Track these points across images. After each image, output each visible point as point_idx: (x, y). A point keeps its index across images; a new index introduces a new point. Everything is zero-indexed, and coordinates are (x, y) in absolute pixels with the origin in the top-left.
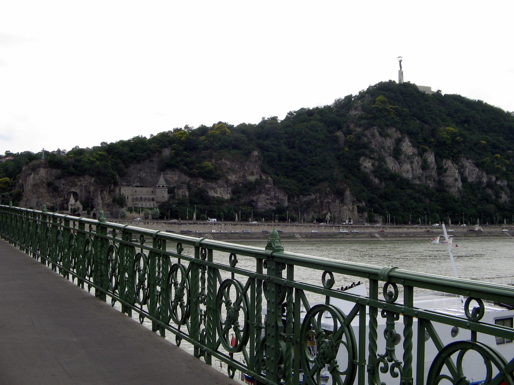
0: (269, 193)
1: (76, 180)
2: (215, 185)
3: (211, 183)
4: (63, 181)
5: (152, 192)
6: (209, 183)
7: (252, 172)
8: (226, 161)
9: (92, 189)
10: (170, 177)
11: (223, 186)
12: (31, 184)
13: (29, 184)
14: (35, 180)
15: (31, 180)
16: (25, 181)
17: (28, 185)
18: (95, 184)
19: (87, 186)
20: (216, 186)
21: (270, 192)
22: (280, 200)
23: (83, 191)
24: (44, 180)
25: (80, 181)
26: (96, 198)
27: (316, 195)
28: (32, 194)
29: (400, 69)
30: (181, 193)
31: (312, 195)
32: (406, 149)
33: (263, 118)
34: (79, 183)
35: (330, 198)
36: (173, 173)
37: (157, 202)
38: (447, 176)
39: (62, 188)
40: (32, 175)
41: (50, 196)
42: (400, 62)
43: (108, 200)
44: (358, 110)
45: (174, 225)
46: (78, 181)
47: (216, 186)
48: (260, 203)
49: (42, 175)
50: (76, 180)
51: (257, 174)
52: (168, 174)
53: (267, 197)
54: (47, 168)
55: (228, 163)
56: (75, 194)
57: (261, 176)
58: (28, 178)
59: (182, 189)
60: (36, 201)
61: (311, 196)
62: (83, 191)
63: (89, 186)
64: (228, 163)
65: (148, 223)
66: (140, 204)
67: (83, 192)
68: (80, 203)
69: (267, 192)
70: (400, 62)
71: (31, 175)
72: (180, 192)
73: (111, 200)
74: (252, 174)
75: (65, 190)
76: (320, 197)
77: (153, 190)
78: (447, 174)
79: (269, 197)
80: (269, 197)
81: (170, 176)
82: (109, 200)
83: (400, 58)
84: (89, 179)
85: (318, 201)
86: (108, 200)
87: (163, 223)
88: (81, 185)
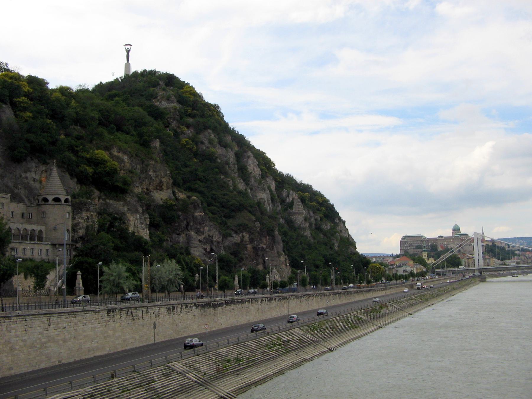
0: (201, 229)
2: (124, 206)
3: (115, 200)
5: (23, 215)
6: (111, 202)
7: (161, 182)
8: (120, 155)
10: (34, 180)
11: (137, 211)
20: (126, 209)
21: (204, 227)
22: (215, 244)
27: (241, 235)
29: (126, 62)
30: (82, 221)
31: (234, 235)
32: (253, 169)
33: (101, 83)
35: (265, 242)
36: (43, 168)
37: (54, 245)
38: (295, 213)
42: (128, 51)
44: (173, 102)
47: (126, 209)
48: (195, 249)
51: (167, 189)
52: (30, 171)
53: (199, 238)
55: (126, 158)
57: (174, 193)
59: (88, 210)
61: (231, 238)
64: (126, 158)
65: (173, 308)
66: (21, 247)
69: (199, 227)
70: (128, 51)
72: (82, 218)
74: (160, 187)
76: (252, 240)
77: (25, 212)
78: (294, 210)
79: (201, 238)
80: (201, 238)
81: (34, 176)
83: (129, 47)
85: (249, 246)
87: (195, 305)
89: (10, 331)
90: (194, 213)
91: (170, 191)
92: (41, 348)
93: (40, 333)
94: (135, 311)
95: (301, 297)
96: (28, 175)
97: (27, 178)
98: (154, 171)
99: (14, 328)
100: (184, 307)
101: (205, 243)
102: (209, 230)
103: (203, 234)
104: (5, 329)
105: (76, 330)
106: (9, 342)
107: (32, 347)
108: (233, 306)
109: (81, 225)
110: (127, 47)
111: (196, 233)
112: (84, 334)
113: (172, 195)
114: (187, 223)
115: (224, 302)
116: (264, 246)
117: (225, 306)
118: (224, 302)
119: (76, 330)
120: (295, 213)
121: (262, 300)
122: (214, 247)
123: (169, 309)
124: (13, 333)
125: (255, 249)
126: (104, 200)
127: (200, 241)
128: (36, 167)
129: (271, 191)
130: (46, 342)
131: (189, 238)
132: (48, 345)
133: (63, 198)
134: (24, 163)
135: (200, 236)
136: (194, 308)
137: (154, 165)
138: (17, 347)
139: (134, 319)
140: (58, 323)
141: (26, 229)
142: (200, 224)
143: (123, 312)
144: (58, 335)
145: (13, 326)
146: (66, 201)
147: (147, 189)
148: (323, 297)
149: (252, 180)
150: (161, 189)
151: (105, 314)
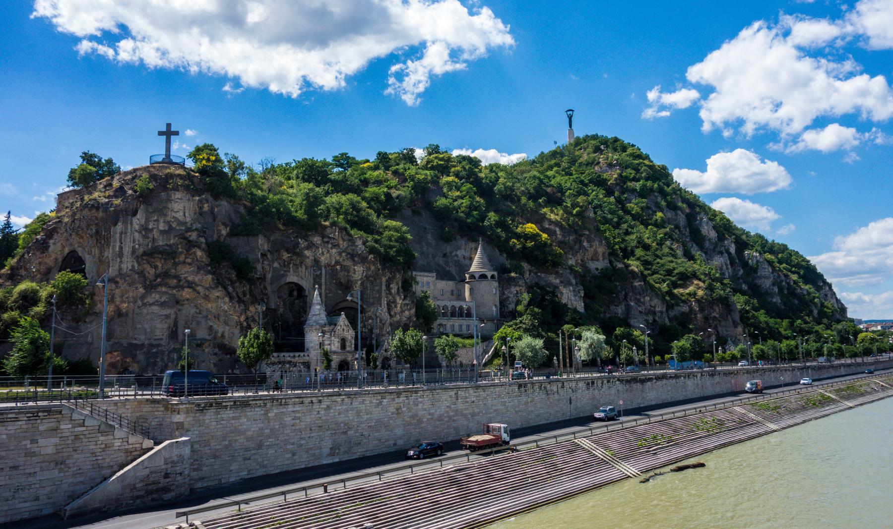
1: (302, 243)
4: (262, 243)
6: (543, 275)
9: (359, 272)
11: (570, 284)
12: (133, 252)
13: (127, 250)
14: (150, 236)
15: (137, 235)
16: (101, 238)
17: (121, 255)
18: (371, 256)
19: (337, 263)
20: (558, 281)
23: (323, 281)
24: (193, 236)
25: (311, 246)
26: (373, 304)
28: (142, 290)
34: (307, 253)
35: (717, 310)
39: (259, 267)
40: (140, 215)
41: (231, 298)
42: (570, 118)
43: (402, 312)
45: (634, 385)
46: (308, 248)
47: (558, 281)
49: (180, 216)
50: (302, 243)
53: (640, 309)
54: (198, 192)
56: (295, 293)
57: (611, 262)
58: (119, 227)
60: (167, 317)
61: (679, 308)
62: (323, 281)
63: (345, 263)
65: (593, 383)
67: (323, 287)
68: (347, 322)
69: (638, 297)
70: (570, 118)
71: (135, 213)
73: (413, 311)
74: (595, 258)
75: (269, 276)
78: (759, 274)
81: (464, 253)
82: (407, 313)
83: (571, 112)
84: (344, 240)
85: (699, 316)
86: (402, 312)
87: (619, 380)
88: (316, 261)
89: (417, 405)
90: (632, 283)
91: (607, 261)
92: (448, 421)
93: (448, 407)
94: (548, 386)
95: (754, 372)
96: (459, 253)
97: (457, 255)
98: (588, 242)
99: (421, 402)
100: (605, 382)
101: (646, 314)
102: (651, 300)
103: (644, 305)
104: (411, 403)
105: (485, 404)
106: (416, 415)
107: (439, 421)
108: (665, 381)
109: (510, 299)
110: (569, 113)
111: (636, 304)
112: (494, 408)
113: (609, 265)
114: (626, 293)
115: (654, 377)
116: (717, 316)
117: (655, 381)
118: (654, 377)
119: (485, 404)
120: (760, 277)
121: (702, 375)
122: (657, 318)
123: (588, 384)
124: (420, 406)
125: (706, 319)
126: (536, 273)
127: (641, 312)
128: (466, 245)
129: (729, 254)
130: (454, 416)
131: (628, 309)
132: (455, 418)
133: (489, 274)
134: (454, 242)
135: (640, 306)
136: (617, 382)
137: (588, 235)
138: (425, 420)
139: (548, 395)
140: (466, 397)
141: (453, 306)
142: (640, 295)
143: (537, 387)
144: (467, 409)
145: (420, 400)
146: (493, 277)
147: (581, 260)
148: (784, 372)
149: (707, 244)
150: (598, 260)
151: (516, 388)
